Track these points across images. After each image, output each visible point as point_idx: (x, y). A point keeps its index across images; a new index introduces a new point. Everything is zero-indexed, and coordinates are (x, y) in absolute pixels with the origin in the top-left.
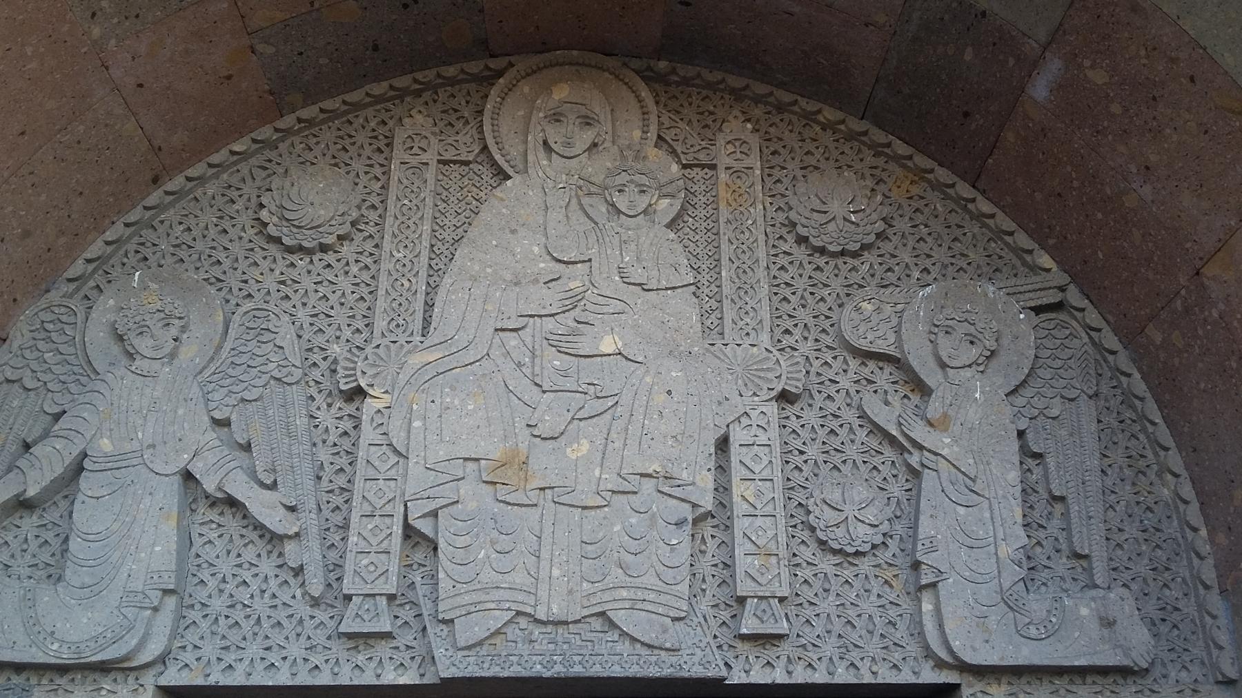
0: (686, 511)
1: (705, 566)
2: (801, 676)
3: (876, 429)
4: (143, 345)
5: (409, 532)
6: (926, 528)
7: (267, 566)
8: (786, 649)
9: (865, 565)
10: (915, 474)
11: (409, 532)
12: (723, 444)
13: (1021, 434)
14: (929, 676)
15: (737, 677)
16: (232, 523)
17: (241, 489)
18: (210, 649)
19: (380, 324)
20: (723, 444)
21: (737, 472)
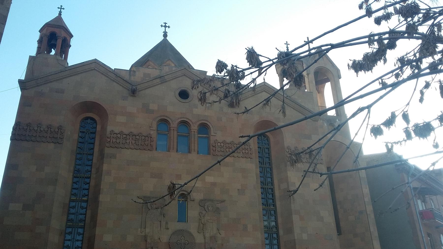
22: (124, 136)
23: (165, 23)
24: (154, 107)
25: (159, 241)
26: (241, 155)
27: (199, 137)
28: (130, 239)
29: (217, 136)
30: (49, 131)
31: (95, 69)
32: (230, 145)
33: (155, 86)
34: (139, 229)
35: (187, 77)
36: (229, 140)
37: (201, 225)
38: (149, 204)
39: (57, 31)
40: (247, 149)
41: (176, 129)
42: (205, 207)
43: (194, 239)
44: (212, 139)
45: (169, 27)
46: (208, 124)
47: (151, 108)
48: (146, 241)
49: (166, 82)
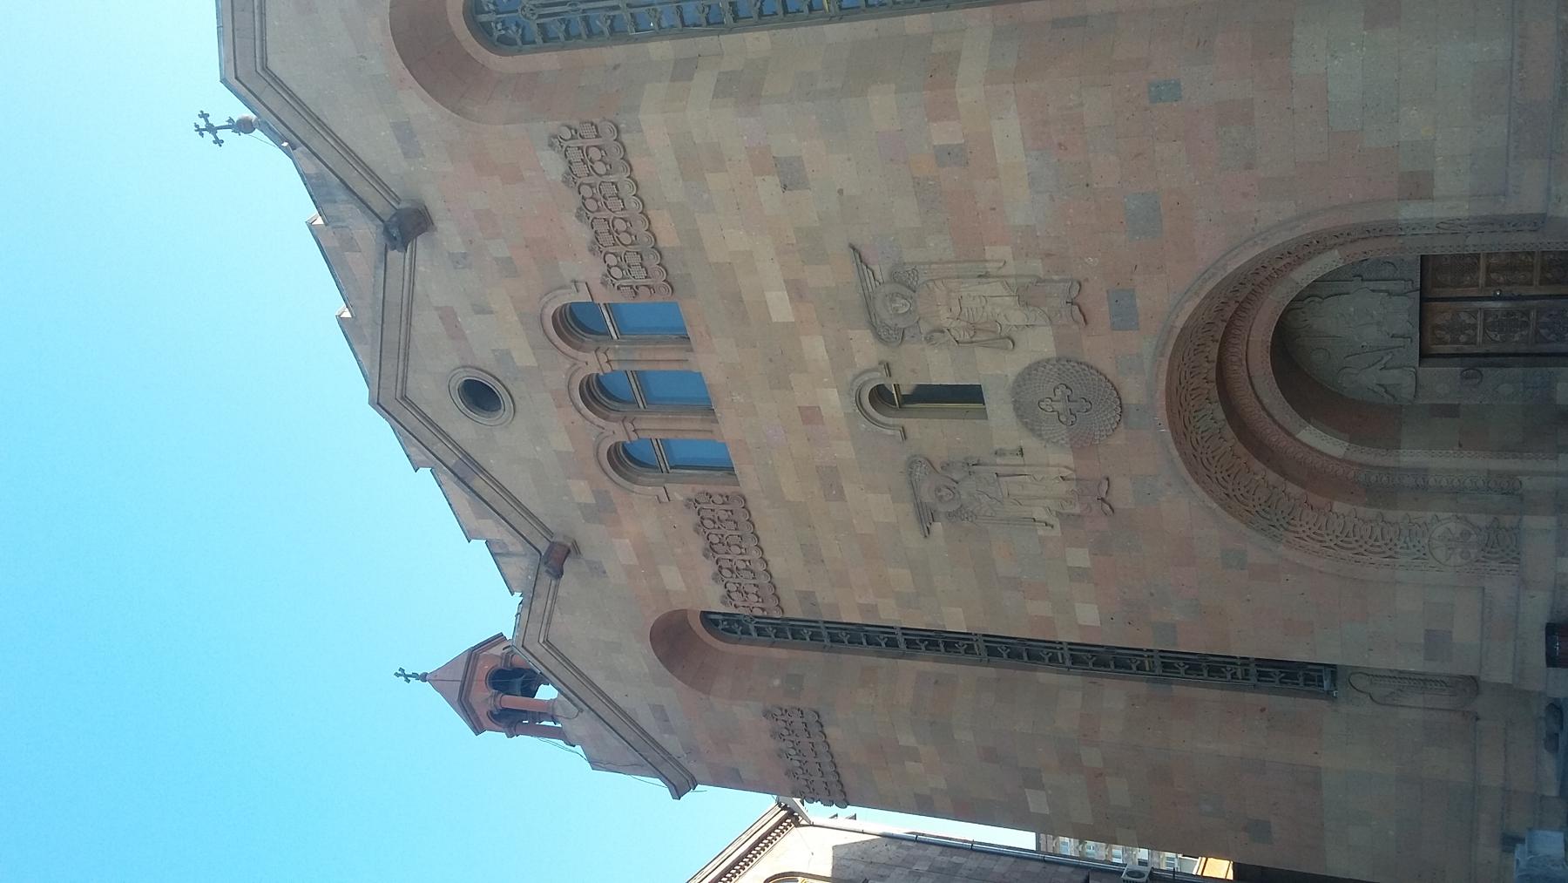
22: (726, 573)
23: (200, 131)
24: (582, 491)
26: (620, 177)
27: (620, 332)
28: (1080, 557)
29: (583, 275)
30: (793, 738)
31: (547, 641)
32: (602, 228)
33: (503, 489)
35: (404, 388)
36: (582, 234)
37: (981, 337)
38: (937, 498)
39: (482, 713)
40: (585, 151)
41: (630, 427)
44: (603, 297)
45: (204, 116)
46: (550, 311)
47: (589, 499)
49: (467, 455)
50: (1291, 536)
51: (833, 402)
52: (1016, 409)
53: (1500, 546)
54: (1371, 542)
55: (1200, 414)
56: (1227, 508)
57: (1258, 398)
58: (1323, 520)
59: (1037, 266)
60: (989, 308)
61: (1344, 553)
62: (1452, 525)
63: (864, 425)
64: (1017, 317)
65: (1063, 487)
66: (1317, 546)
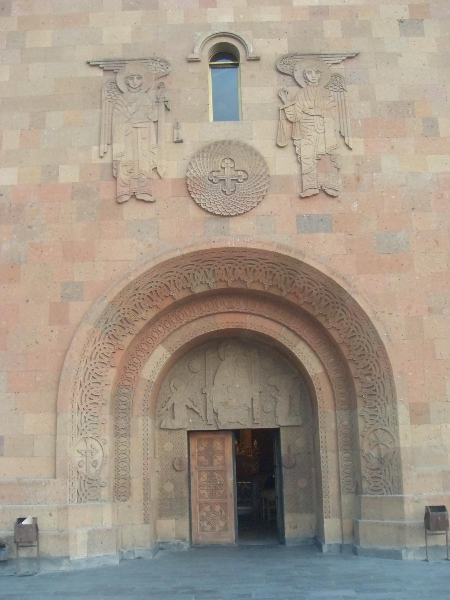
0: (248, 408)
1: (250, 414)
2: (262, 427)
3: (272, 396)
4: (178, 388)
5: (214, 412)
6: (277, 410)
7: (197, 416)
8: (260, 424)
9: (270, 414)
10: (276, 402)
11: (214, 412)
12: (252, 399)
13: (290, 396)
14: (277, 427)
15: (254, 428)
16: (192, 411)
17: (194, 407)
18: (192, 426)
19: (207, 383)
20: (252, 399)
21: (254, 403)
25: (155, 177)
28: (69, 175)
34: (95, 148)
37: (287, 127)
42: (298, 75)
43: (265, 164)
48: (115, 178)
50: (97, 335)
51: (222, 19)
52: (223, 142)
53: (88, 488)
54: (89, 395)
55: (210, 274)
56: (128, 287)
57: (196, 319)
58: (106, 360)
59: (349, 170)
60: (315, 134)
61: (81, 374)
62: (100, 454)
63: (202, 36)
64: (308, 152)
65: (146, 168)
66: (88, 354)
